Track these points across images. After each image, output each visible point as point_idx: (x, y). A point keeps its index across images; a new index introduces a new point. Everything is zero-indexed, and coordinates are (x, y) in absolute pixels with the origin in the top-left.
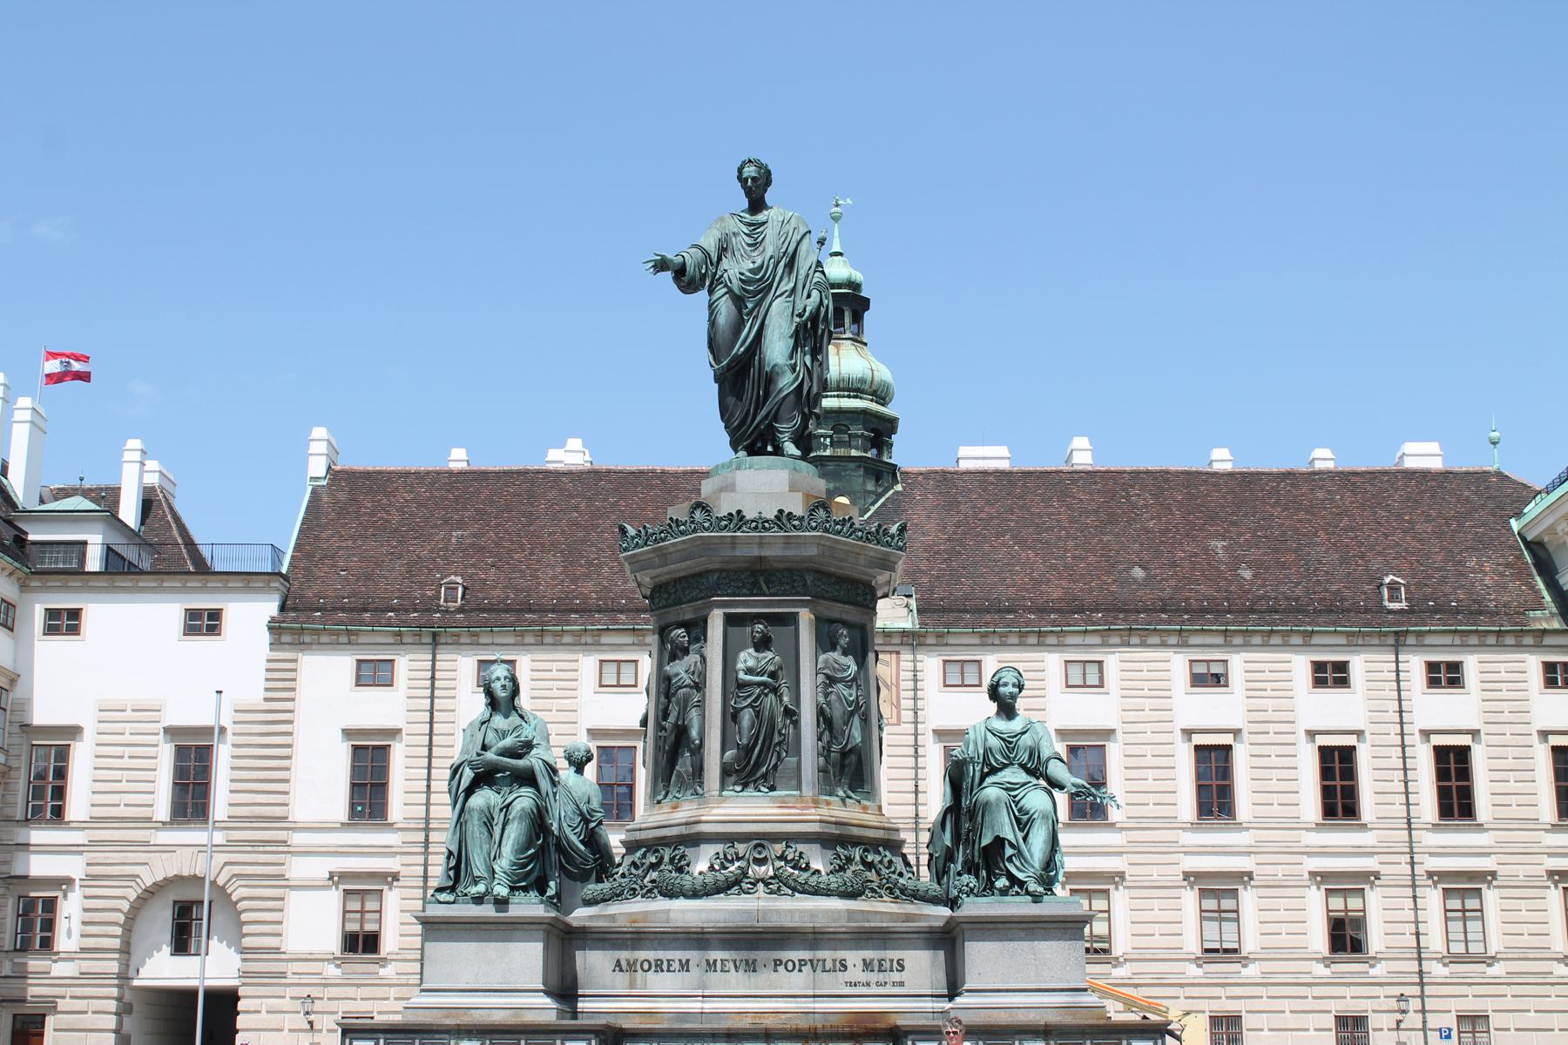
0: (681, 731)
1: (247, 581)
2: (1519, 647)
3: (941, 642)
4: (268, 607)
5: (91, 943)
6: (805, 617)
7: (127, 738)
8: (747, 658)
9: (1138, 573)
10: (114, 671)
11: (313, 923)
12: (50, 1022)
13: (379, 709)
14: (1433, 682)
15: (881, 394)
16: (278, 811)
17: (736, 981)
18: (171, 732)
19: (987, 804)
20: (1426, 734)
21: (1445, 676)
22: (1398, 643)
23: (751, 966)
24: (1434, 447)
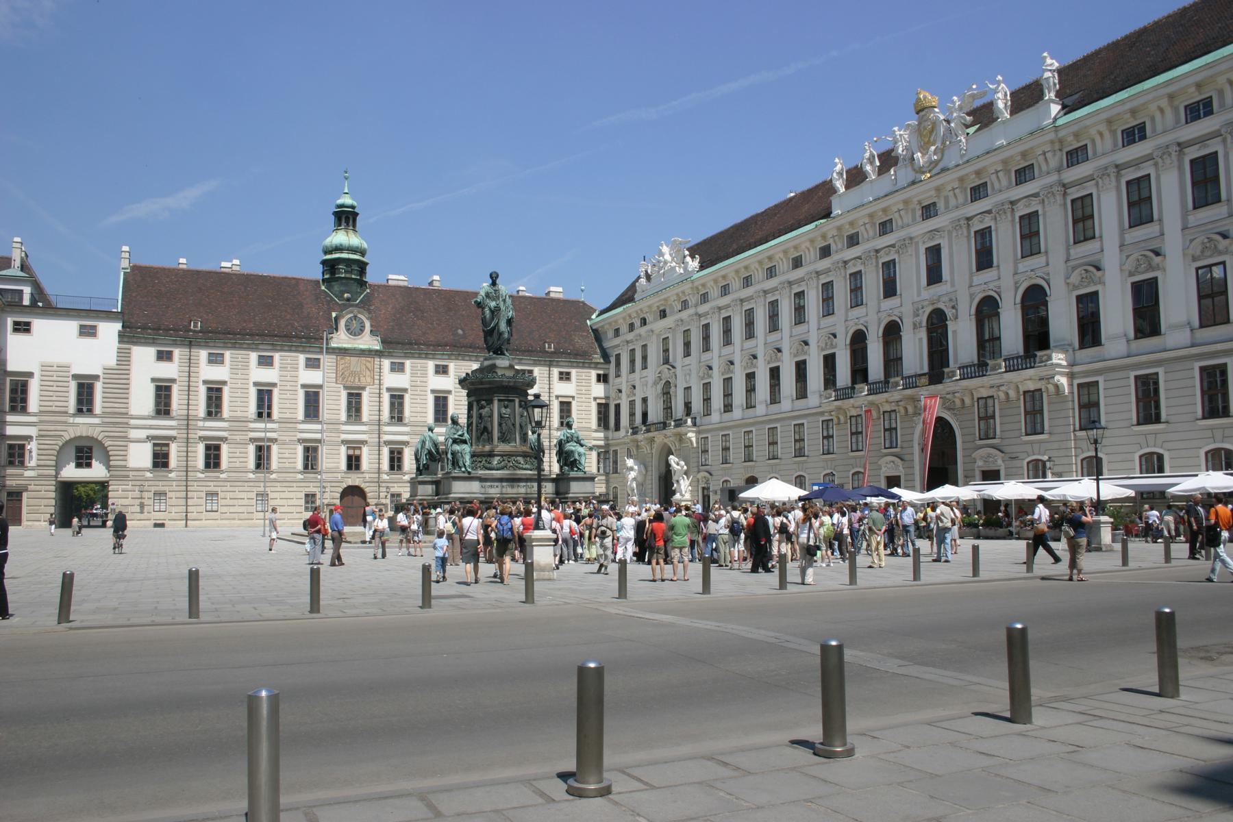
0: (485, 429)
1: (108, 315)
2: (590, 368)
3: (390, 355)
4: (118, 326)
5: (42, 463)
6: (517, 401)
7: (55, 378)
8: (503, 410)
9: (460, 332)
10: (49, 350)
11: (140, 456)
12: (25, 495)
13: (168, 370)
14: (561, 379)
15: (363, 253)
16: (123, 411)
17: (509, 490)
18: (75, 377)
19: (572, 452)
20: (557, 397)
21: (565, 377)
22: (550, 365)
23: (512, 487)
24: (560, 289)
